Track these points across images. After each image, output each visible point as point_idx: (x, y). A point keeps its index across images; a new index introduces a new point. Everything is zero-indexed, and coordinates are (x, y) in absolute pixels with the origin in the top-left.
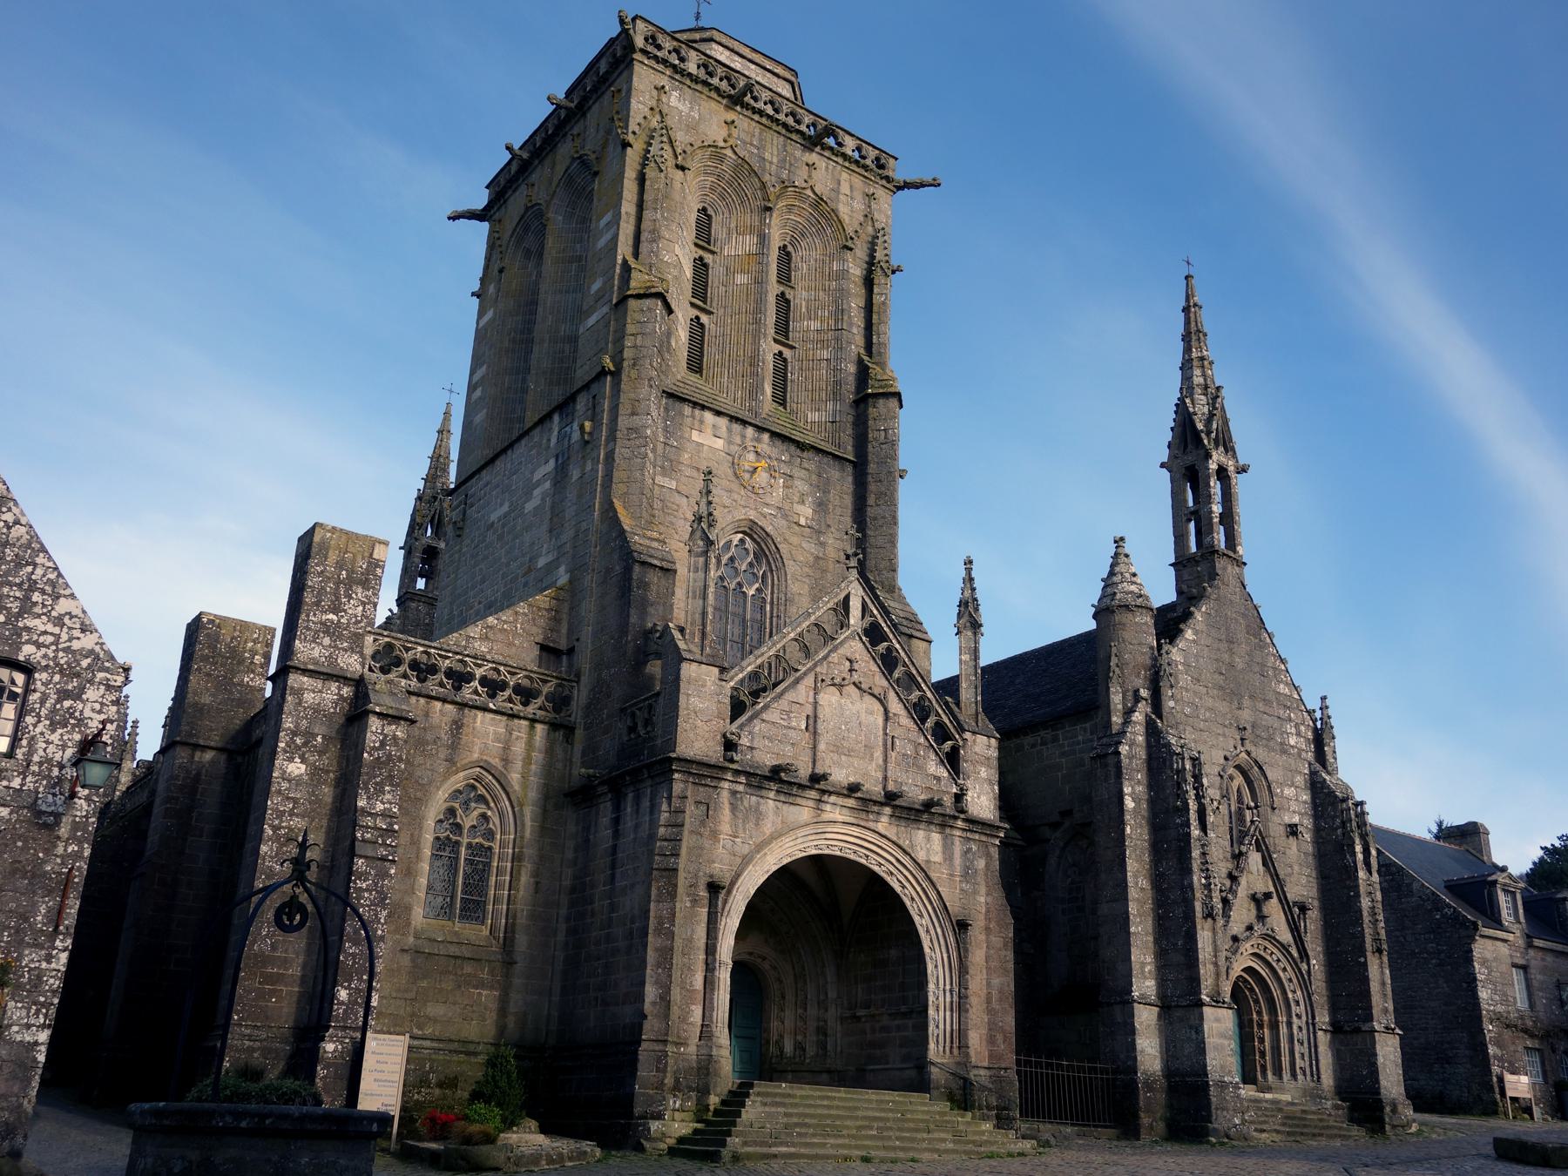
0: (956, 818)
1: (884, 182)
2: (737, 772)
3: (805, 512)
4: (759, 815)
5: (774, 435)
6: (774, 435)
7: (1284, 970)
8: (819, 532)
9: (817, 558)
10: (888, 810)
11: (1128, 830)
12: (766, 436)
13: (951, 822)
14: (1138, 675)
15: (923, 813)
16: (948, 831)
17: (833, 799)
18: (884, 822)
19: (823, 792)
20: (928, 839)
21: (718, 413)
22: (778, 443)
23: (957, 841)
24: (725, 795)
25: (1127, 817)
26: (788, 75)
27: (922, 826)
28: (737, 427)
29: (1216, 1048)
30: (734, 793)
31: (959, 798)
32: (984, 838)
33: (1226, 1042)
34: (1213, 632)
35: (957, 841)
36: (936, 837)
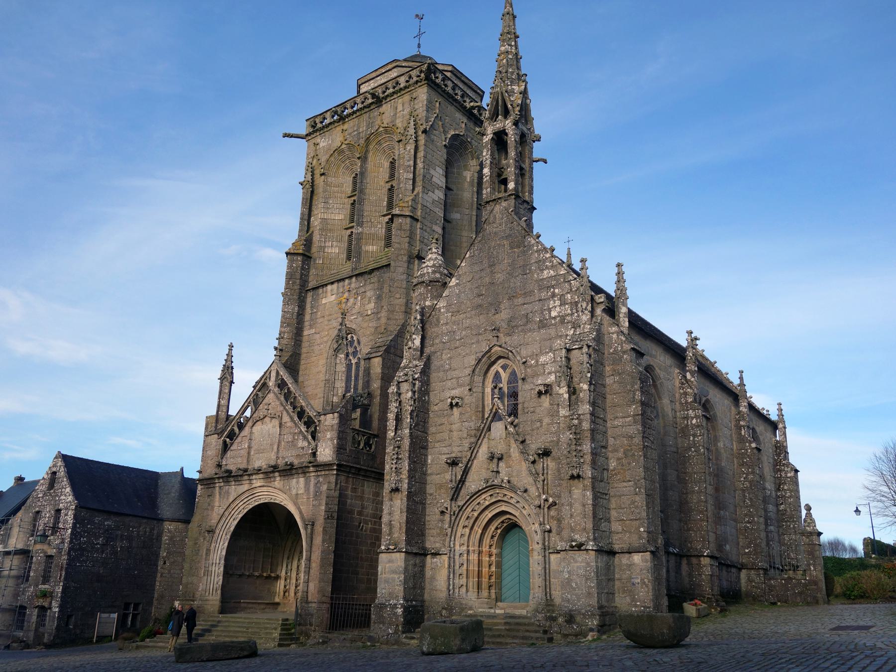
0: (309, 467)
1: (419, 84)
2: (219, 478)
3: (370, 307)
4: (228, 493)
5: (357, 275)
6: (357, 275)
8: (378, 313)
9: (377, 328)
10: (277, 474)
12: (354, 279)
13: (307, 470)
15: (288, 471)
16: (308, 475)
17: (254, 477)
18: (278, 482)
19: (249, 475)
20: (297, 482)
21: (332, 283)
22: (360, 278)
23: (312, 479)
24: (217, 489)
26: (394, 64)
27: (296, 476)
28: (341, 284)
29: (386, 581)
30: (220, 487)
31: (314, 454)
32: (327, 472)
33: (396, 576)
34: (477, 268)
35: (312, 479)
36: (302, 480)
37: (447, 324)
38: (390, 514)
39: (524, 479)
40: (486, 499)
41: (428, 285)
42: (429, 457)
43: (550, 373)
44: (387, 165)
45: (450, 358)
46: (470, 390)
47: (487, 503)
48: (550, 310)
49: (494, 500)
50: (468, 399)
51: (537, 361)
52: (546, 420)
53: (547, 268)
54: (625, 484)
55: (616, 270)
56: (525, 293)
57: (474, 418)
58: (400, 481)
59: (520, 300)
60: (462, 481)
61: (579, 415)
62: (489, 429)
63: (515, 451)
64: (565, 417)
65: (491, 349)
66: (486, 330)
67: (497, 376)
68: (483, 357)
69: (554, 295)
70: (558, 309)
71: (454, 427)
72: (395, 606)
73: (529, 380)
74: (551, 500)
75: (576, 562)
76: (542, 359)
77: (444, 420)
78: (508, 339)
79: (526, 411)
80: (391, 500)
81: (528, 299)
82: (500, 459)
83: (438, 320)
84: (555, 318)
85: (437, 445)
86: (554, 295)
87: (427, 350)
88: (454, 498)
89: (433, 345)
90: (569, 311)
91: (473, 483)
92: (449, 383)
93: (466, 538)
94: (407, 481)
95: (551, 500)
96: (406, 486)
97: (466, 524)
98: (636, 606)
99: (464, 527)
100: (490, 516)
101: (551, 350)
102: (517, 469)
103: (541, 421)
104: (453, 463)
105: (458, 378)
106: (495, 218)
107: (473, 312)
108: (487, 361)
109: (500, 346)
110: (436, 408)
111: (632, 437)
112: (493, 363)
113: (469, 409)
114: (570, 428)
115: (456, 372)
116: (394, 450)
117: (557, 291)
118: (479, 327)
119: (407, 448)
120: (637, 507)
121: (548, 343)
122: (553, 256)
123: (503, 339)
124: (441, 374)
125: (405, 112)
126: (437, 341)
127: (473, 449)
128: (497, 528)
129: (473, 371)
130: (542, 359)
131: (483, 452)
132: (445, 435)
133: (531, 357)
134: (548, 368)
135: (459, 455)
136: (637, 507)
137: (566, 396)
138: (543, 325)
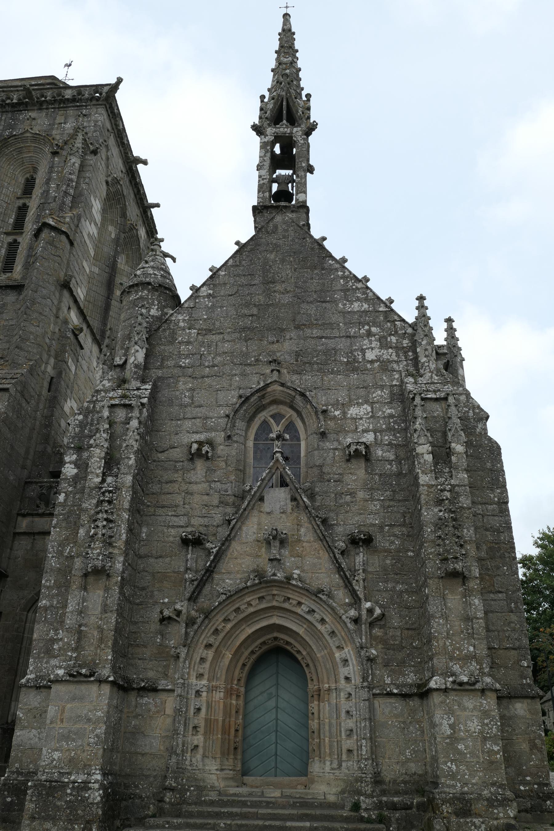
1: (94, 102)
7: (323, 621)
11: (61, 498)
14: (122, 348)
25: (64, 485)
37: (188, 343)
38: (80, 613)
39: (323, 575)
40: (252, 603)
41: (155, 289)
42: (144, 530)
43: (364, 431)
44: (22, 180)
45: (192, 390)
46: (229, 437)
47: (251, 610)
48: (363, 351)
49: (263, 605)
50: (221, 450)
51: (344, 413)
52: (361, 495)
53: (358, 299)
54: (492, 595)
55: (445, 325)
56: (324, 324)
57: (233, 478)
58: (110, 556)
59: (316, 332)
60: (210, 572)
61: (454, 486)
62: (262, 499)
63: (306, 533)
64: (430, 486)
65: (267, 386)
66: (257, 360)
67: (265, 427)
68: (252, 395)
69: (369, 334)
70: (376, 352)
71: (194, 488)
72: (85, 786)
73: (332, 436)
74: (378, 611)
75: (465, 709)
76: (353, 411)
77: (177, 476)
78: (295, 377)
79: (327, 477)
80: (85, 589)
81: (327, 333)
82: (283, 542)
83: (173, 334)
84: (372, 362)
85: (160, 511)
86: (369, 334)
87: (155, 373)
88: (193, 598)
89: (161, 367)
90: (394, 357)
91: (229, 577)
92: (188, 424)
93: (207, 665)
94: (121, 559)
95: (378, 611)
96: (119, 566)
97: (211, 640)
98: (525, 783)
99: (209, 646)
100: (250, 631)
101: (367, 402)
102: (311, 564)
103: (352, 494)
104: (193, 542)
105: (206, 418)
106: (276, 227)
107: (237, 335)
108: (253, 404)
109: (283, 385)
110: (162, 457)
111: (499, 532)
112: (263, 408)
113: (223, 464)
114: (439, 502)
115: (203, 410)
116: (97, 506)
117: (374, 329)
118: (246, 355)
119: (126, 505)
120: (514, 630)
121: (362, 392)
122: (368, 288)
123: (287, 377)
124: (175, 410)
125: (68, 125)
126: (170, 363)
127: (233, 525)
128: (253, 652)
129: (236, 412)
130: (353, 411)
131: (252, 529)
132: (179, 500)
133: (336, 405)
134: (363, 425)
135: (202, 529)
136: (514, 630)
137: (429, 458)
138: (353, 366)
